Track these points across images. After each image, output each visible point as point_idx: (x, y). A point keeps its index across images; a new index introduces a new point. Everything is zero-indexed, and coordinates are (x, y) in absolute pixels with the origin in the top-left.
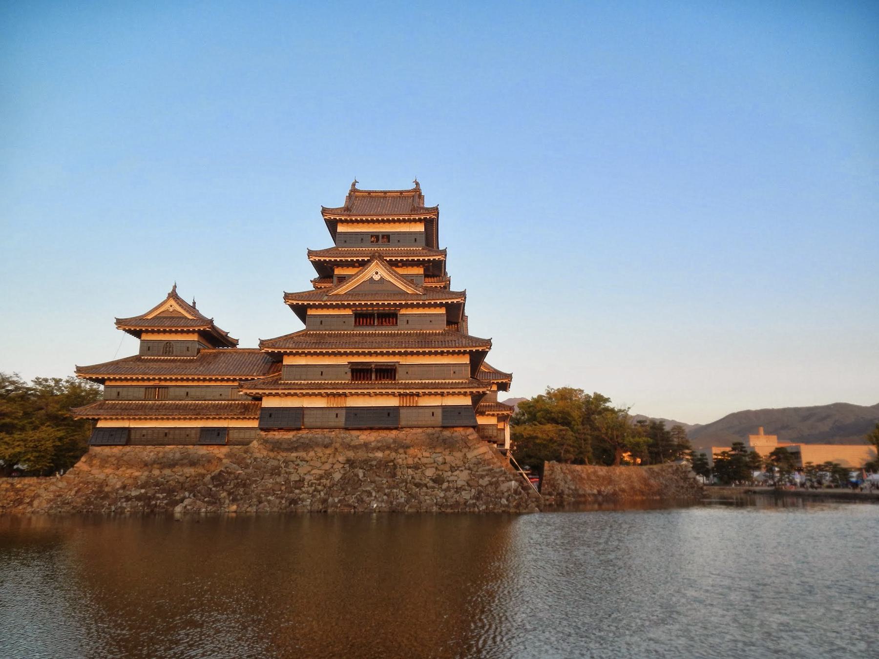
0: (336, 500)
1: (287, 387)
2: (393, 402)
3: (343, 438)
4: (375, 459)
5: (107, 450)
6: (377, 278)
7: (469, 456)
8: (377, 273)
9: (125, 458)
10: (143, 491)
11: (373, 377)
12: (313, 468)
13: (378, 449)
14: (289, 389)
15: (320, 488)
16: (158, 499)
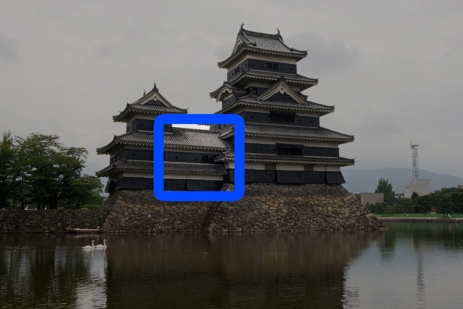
0: (292, 224)
1: (249, 157)
2: (301, 169)
3: (276, 189)
4: (298, 201)
5: (132, 193)
6: (282, 92)
7: (345, 199)
8: (282, 89)
9: (144, 198)
10: (167, 219)
11: (290, 153)
12: (271, 206)
13: (298, 196)
14: (251, 158)
15: (279, 217)
16: (178, 224)
